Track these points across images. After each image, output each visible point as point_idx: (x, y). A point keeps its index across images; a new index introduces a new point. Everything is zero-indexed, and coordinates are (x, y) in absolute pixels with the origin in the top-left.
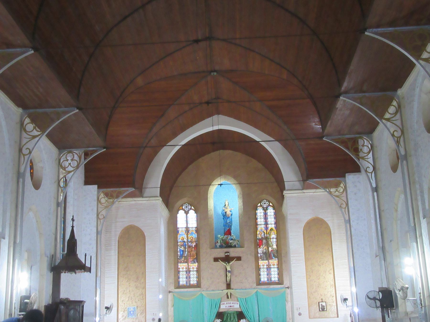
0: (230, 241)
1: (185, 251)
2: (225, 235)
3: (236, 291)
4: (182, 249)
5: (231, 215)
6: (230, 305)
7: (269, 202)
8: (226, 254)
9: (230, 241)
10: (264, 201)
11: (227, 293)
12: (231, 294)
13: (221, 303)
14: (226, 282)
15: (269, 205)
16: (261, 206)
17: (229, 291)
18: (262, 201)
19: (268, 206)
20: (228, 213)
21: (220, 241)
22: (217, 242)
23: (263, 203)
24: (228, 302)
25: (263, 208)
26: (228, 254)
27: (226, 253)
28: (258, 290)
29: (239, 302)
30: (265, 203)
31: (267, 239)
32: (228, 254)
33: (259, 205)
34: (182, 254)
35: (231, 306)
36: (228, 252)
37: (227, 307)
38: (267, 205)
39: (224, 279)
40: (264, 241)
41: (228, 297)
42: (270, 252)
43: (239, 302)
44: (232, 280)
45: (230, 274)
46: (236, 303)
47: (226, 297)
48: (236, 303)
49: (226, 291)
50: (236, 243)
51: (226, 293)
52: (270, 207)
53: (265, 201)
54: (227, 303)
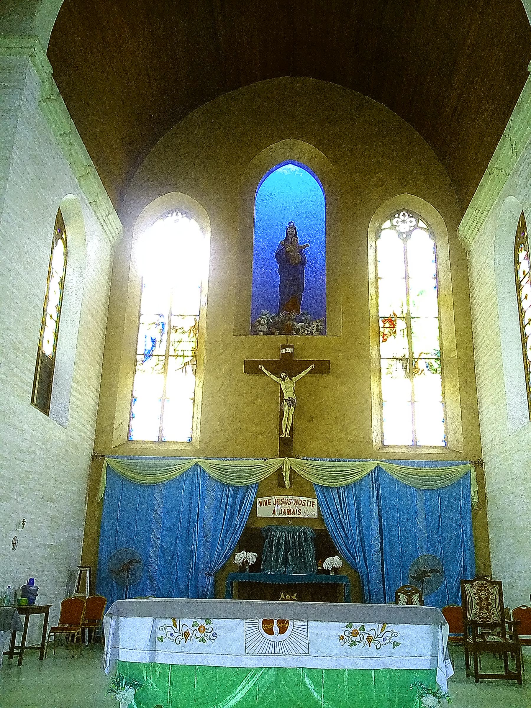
0: (295, 323)
1: (161, 341)
2: (281, 311)
3: (307, 462)
4: (155, 333)
5: (303, 262)
6: (287, 507)
7: (418, 217)
8: (283, 351)
9: (295, 323)
10: (402, 213)
11: (280, 470)
12: (291, 470)
13: (259, 500)
14: (277, 432)
15: (416, 227)
16: (393, 227)
17: (289, 462)
18: (397, 216)
19: (413, 230)
20: (295, 256)
21: (268, 321)
22: (260, 322)
23: (399, 220)
24: (280, 497)
25: (400, 234)
26: (291, 350)
27: (283, 347)
28: (383, 465)
29: (316, 501)
30: (404, 221)
31: (408, 318)
32: (291, 350)
33: (387, 224)
34: (152, 348)
35: (289, 512)
36: (291, 347)
37: (277, 515)
38: (410, 227)
39: (272, 424)
40: (400, 325)
41: (282, 484)
42: (416, 356)
43: (316, 501)
44: (297, 428)
45: (292, 409)
46: (306, 503)
47: (276, 480)
48: (306, 503)
49: (275, 462)
50: (316, 327)
51: (277, 467)
52: (417, 232)
53: (404, 215)
54: (277, 502)
